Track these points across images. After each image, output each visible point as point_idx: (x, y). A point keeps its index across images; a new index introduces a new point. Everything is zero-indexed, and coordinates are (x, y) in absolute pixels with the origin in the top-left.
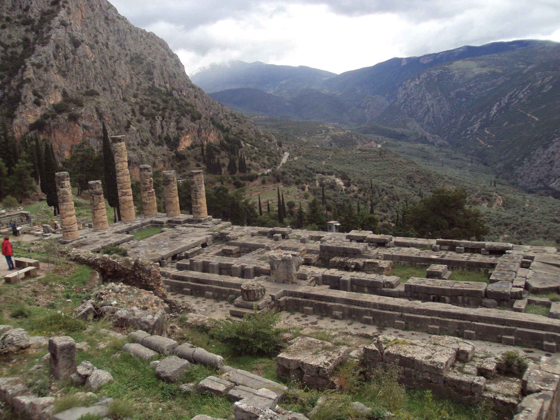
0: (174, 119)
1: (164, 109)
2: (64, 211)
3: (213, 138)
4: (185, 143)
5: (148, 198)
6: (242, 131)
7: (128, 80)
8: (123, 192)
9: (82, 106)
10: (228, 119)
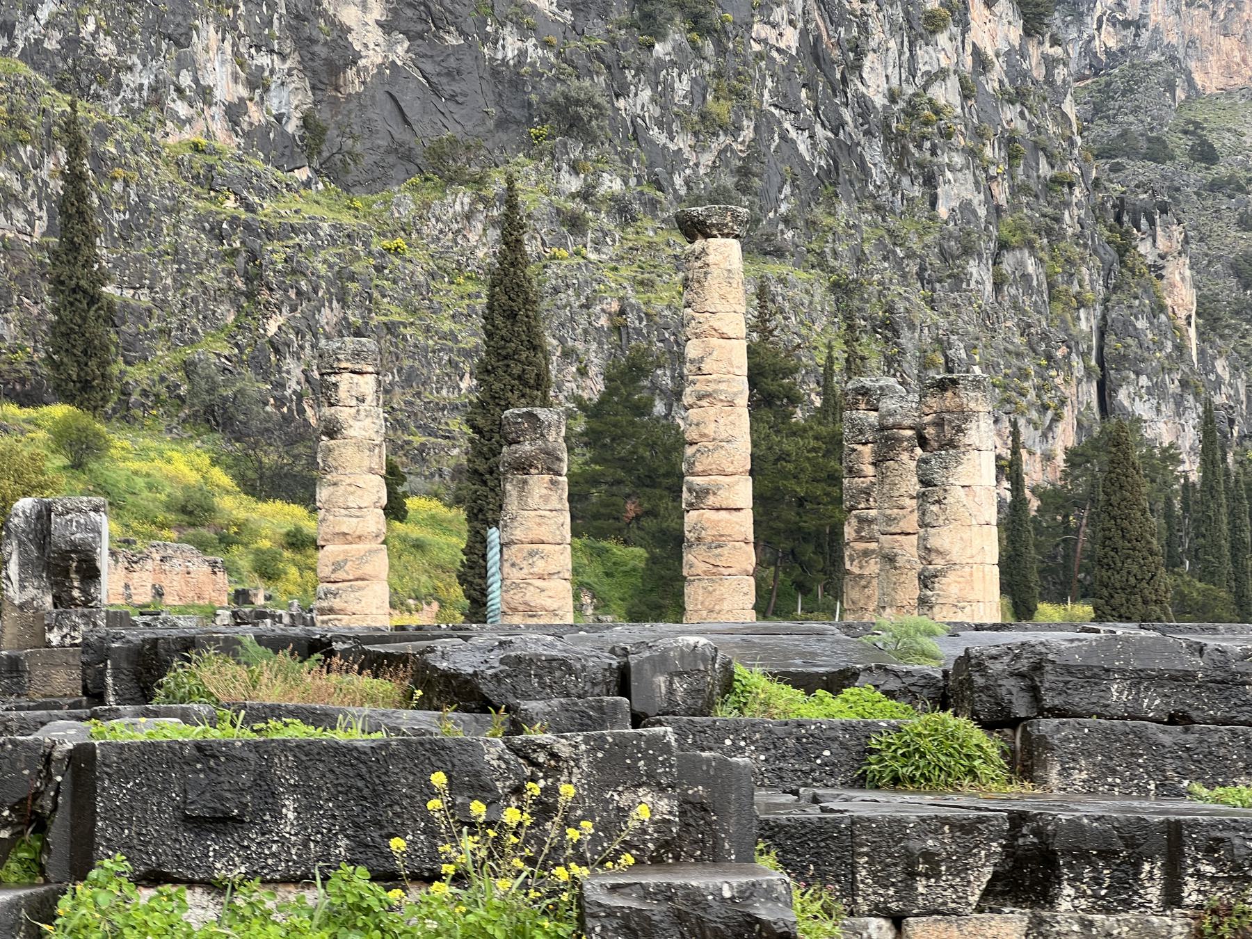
5: (860, 546)
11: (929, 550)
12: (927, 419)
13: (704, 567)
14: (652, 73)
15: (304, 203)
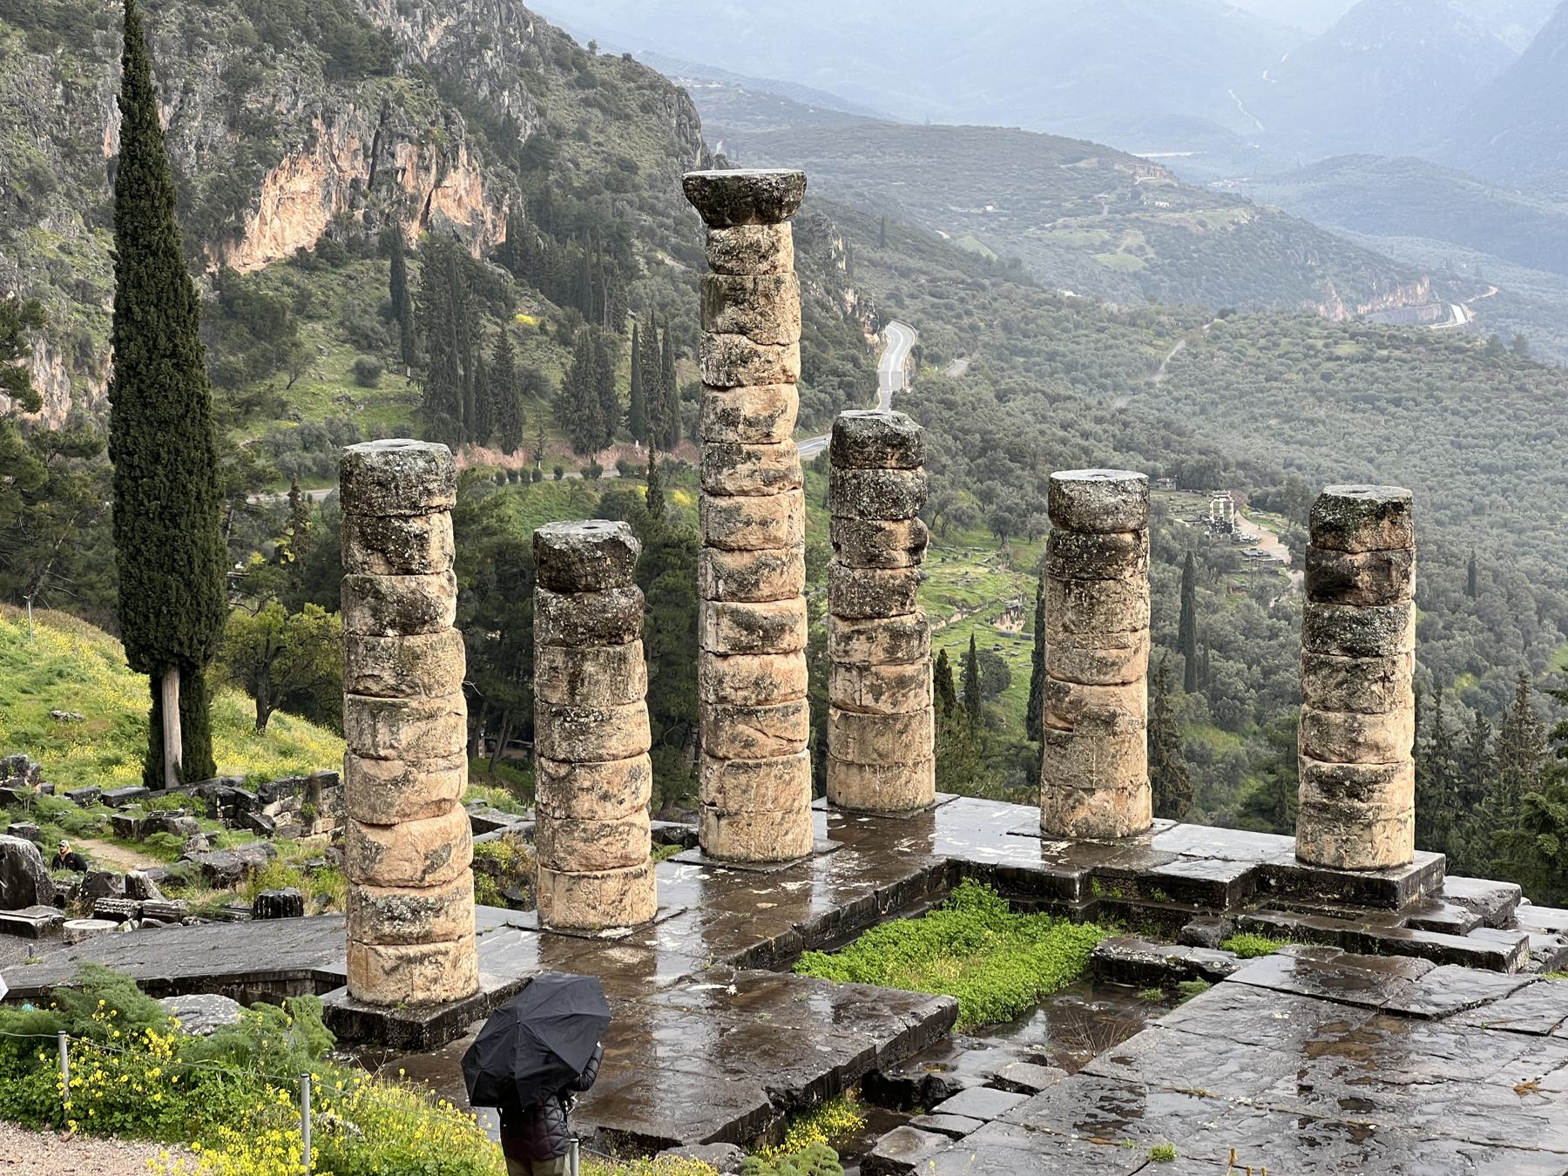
0: (214, 59)
2: (397, 768)
5: (889, 671)
6: (629, 166)
8: (747, 624)
10: (539, 87)
11: (1356, 744)
12: (1359, 559)
13: (772, 744)
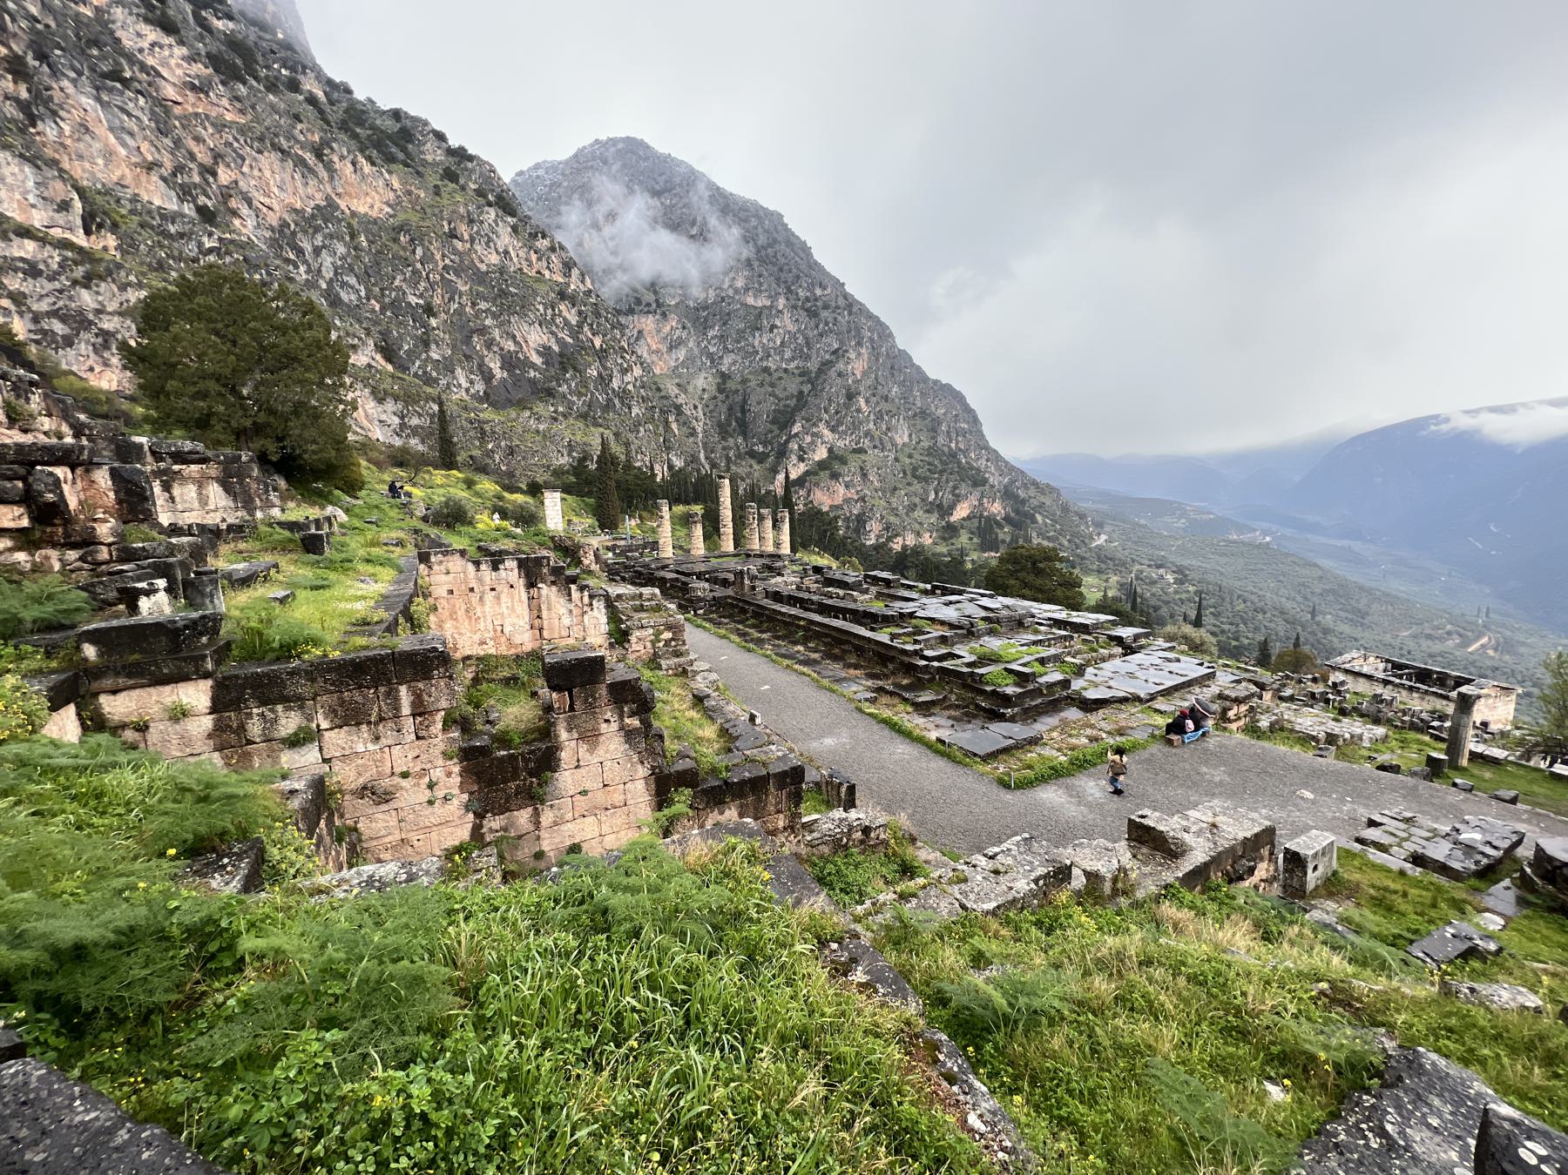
1: (941, 472)
3: (996, 508)
4: (961, 512)
7: (906, 439)
9: (845, 463)
14: (566, 381)
15: (488, 414)
